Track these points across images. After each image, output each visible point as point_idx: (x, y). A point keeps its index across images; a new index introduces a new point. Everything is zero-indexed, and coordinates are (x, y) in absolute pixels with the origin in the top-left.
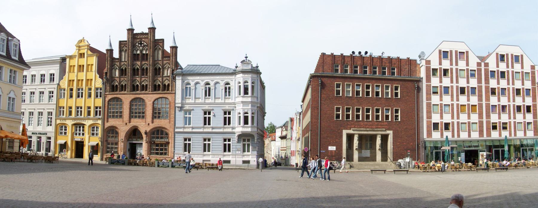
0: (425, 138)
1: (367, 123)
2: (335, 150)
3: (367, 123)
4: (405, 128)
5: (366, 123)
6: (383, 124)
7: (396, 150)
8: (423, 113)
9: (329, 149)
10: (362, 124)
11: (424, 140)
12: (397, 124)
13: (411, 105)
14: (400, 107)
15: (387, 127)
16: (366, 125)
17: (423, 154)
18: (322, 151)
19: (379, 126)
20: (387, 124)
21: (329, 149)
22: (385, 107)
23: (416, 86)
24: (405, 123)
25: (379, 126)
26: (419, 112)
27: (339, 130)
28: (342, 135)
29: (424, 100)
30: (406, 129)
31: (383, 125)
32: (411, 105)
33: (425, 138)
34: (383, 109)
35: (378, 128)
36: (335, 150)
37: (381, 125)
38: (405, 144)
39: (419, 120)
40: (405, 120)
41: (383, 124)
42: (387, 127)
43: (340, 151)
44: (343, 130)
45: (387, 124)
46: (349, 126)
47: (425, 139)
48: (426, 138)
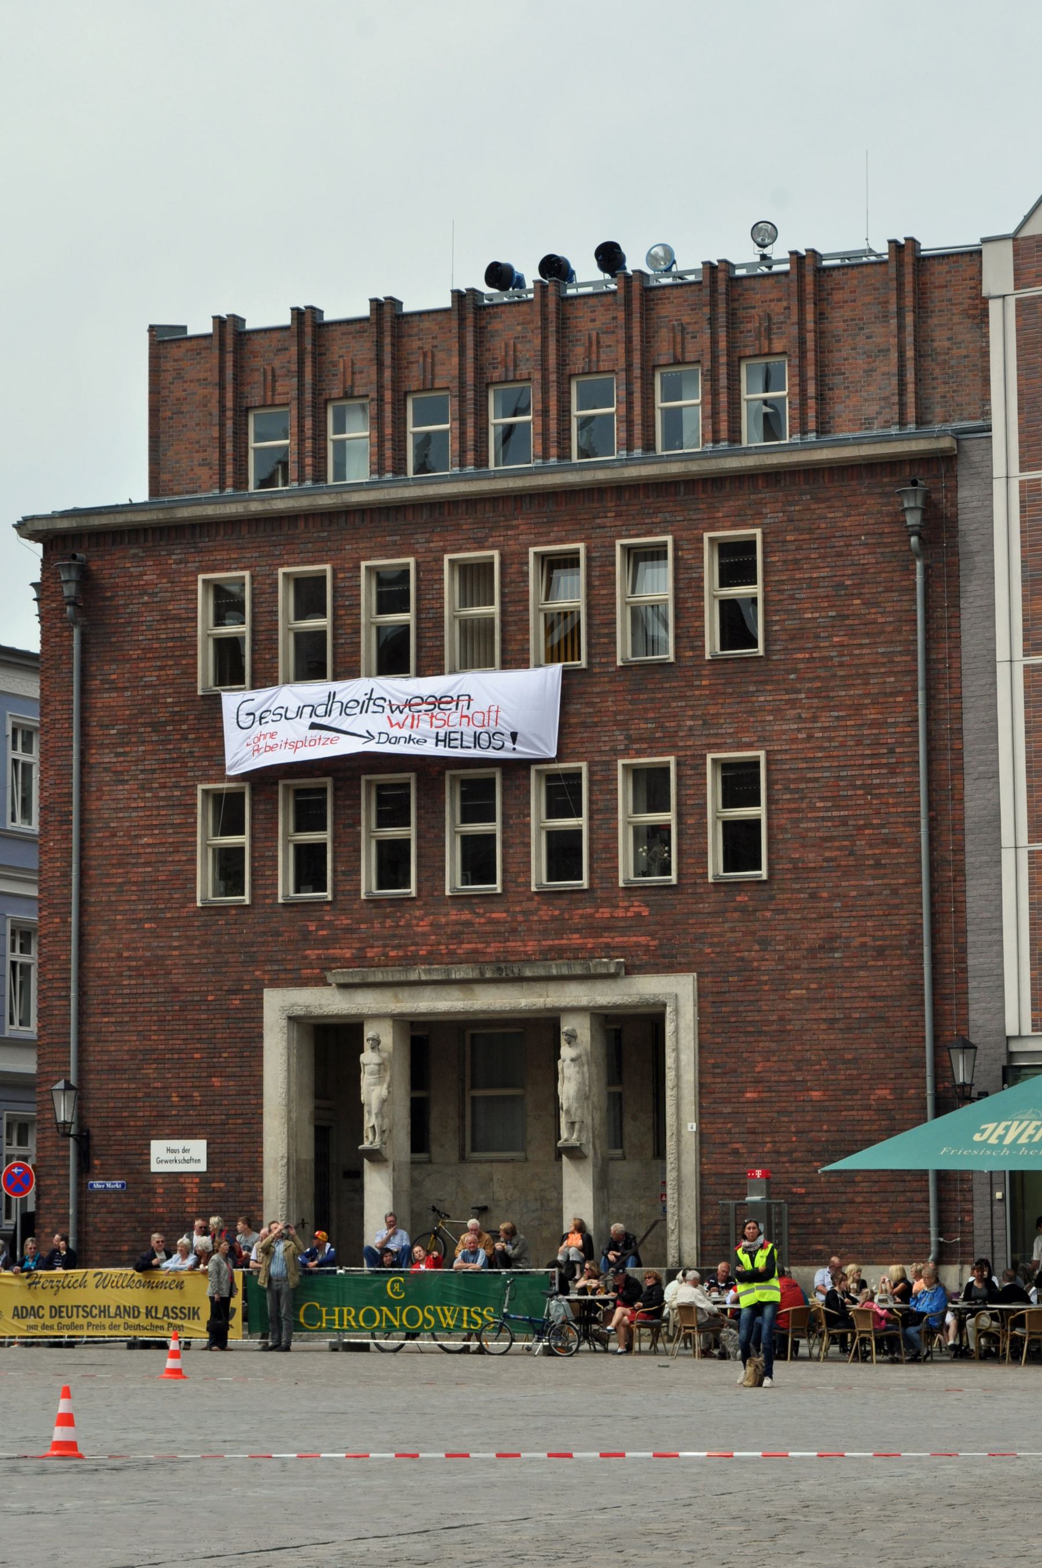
0: (1011, 1030)
1: (466, 916)
2: (202, 1167)
3: (466, 916)
4: (813, 936)
5: (454, 915)
6: (605, 912)
7: (736, 1152)
8: (994, 775)
9: (155, 1167)
10: (423, 927)
11: (1011, 1055)
12: (743, 910)
13: (871, 714)
14: (761, 741)
15: (643, 940)
16: (457, 937)
17: (999, 1195)
18: (97, 1185)
19: (576, 939)
20: (645, 912)
21: (155, 1167)
22: (626, 753)
23: (913, 519)
24: (813, 896)
25: (576, 939)
26: (959, 770)
27: (230, 992)
28: (261, 1036)
29: (1002, 653)
30: (828, 944)
31: (608, 929)
32: (871, 714)
33: (1011, 1030)
34: (611, 766)
35: (560, 953)
36: (202, 1167)
37: (594, 929)
38: (816, 1095)
39: (960, 849)
40: (812, 857)
41: (605, 912)
42: (643, 940)
43: (240, 1180)
44: (265, 990)
45: (645, 912)
46: (312, 954)
47: (1015, 1047)
48: (1027, 1030)
